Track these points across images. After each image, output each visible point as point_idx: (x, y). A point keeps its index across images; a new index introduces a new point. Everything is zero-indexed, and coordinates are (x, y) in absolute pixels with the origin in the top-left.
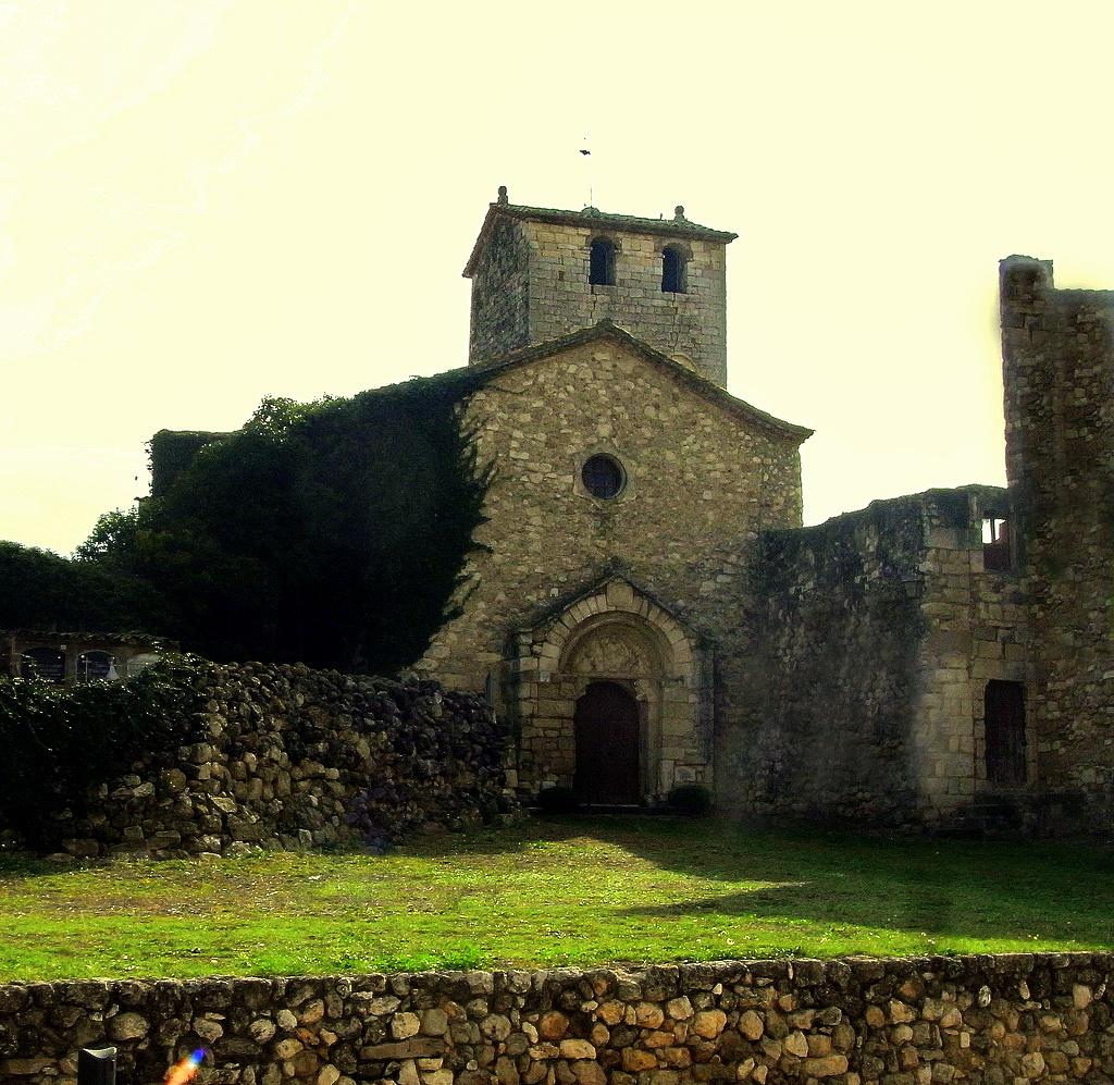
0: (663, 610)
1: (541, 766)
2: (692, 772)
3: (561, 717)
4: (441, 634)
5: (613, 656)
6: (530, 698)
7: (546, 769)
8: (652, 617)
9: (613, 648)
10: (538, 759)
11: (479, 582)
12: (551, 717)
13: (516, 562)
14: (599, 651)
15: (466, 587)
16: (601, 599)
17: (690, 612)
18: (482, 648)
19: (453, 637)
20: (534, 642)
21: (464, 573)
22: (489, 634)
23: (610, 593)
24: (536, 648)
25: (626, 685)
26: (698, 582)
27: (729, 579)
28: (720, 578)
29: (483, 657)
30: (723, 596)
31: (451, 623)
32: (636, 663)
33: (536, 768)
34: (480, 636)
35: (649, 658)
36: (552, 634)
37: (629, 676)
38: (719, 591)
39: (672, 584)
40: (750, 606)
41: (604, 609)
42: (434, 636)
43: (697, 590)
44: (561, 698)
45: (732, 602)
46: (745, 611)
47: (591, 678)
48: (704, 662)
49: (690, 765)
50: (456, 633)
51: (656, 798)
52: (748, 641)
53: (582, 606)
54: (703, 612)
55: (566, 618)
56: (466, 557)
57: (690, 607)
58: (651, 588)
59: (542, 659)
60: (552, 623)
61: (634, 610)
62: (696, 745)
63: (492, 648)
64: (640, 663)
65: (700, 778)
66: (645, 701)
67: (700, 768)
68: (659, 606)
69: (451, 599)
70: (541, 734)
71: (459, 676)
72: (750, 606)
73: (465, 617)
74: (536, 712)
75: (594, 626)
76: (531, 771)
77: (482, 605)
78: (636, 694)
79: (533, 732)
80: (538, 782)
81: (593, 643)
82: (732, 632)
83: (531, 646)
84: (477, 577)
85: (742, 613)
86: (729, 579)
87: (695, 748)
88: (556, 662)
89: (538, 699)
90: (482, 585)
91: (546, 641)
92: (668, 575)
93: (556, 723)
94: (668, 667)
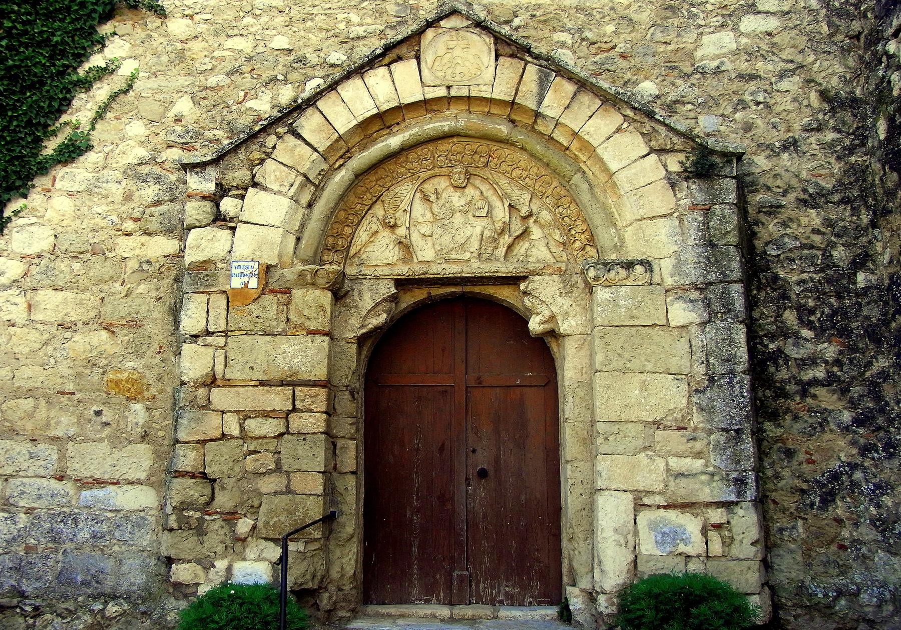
0: (583, 85)
1: (231, 517)
2: (691, 525)
3: (290, 382)
4: (36, 198)
5: (458, 219)
6: (209, 333)
7: (244, 525)
8: (552, 106)
9: (458, 200)
10: (224, 500)
11: (133, 78)
12: (262, 384)
13: (223, 31)
14: (419, 209)
15: (101, 92)
16: (405, 70)
17: (671, 108)
18: (129, 226)
19: (61, 205)
20: (222, 191)
21: (97, 60)
22: (150, 192)
23: (428, 57)
24: (228, 205)
25: (505, 294)
26: (690, 37)
27: (773, 24)
28: (750, 23)
29: (128, 247)
30: (760, 64)
31: (60, 172)
32: (525, 234)
33: (216, 525)
34: (128, 197)
35: (558, 222)
36: (270, 164)
37: (504, 269)
38: (751, 54)
39: (621, 47)
40: (835, 81)
41: (412, 93)
42: (16, 204)
43: (690, 55)
44: (292, 329)
45: (782, 75)
46: (824, 95)
47: (403, 284)
48: (707, 211)
49: (687, 506)
50: (70, 194)
51: (591, 596)
52: (837, 168)
53: (351, 90)
54: (708, 104)
55: (309, 124)
56: (106, 29)
57: (672, 96)
58: (566, 57)
59: (241, 229)
60: (271, 140)
61: (502, 92)
62: (698, 446)
63: (153, 226)
64: (536, 233)
65: (716, 548)
66: (553, 334)
67: (717, 516)
68: (570, 76)
69: (64, 118)
70: (235, 431)
71: (69, 295)
72: (835, 81)
73: (91, 157)
74: (219, 368)
75: (394, 141)
76: (200, 531)
77: (137, 129)
78: (530, 312)
79: (212, 425)
80: (221, 565)
81: (405, 190)
82: (790, 145)
83: (215, 199)
84: (127, 69)
85: (814, 97)
86: (773, 24)
87: (699, 455)
88: (276, 235)
89: (225, 333)
90: (138, 85)
91: (255, 185)
92: (610, 28)
93: (278, 400)
94: (607, 237)
